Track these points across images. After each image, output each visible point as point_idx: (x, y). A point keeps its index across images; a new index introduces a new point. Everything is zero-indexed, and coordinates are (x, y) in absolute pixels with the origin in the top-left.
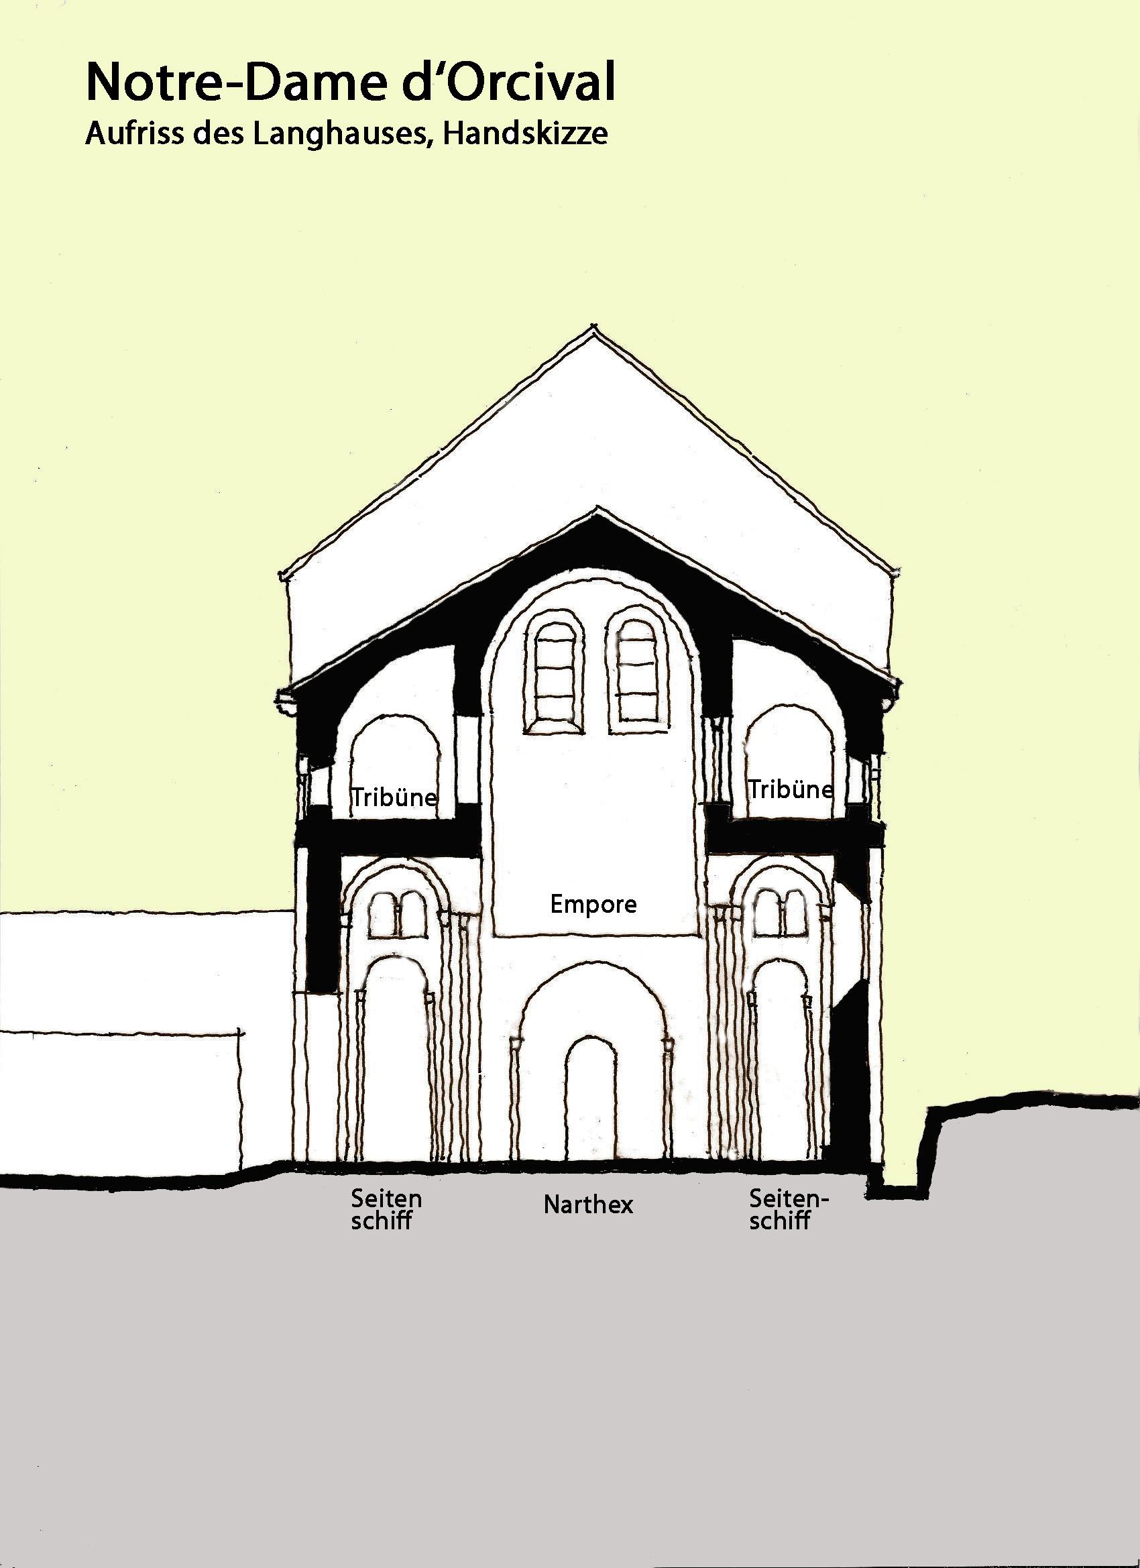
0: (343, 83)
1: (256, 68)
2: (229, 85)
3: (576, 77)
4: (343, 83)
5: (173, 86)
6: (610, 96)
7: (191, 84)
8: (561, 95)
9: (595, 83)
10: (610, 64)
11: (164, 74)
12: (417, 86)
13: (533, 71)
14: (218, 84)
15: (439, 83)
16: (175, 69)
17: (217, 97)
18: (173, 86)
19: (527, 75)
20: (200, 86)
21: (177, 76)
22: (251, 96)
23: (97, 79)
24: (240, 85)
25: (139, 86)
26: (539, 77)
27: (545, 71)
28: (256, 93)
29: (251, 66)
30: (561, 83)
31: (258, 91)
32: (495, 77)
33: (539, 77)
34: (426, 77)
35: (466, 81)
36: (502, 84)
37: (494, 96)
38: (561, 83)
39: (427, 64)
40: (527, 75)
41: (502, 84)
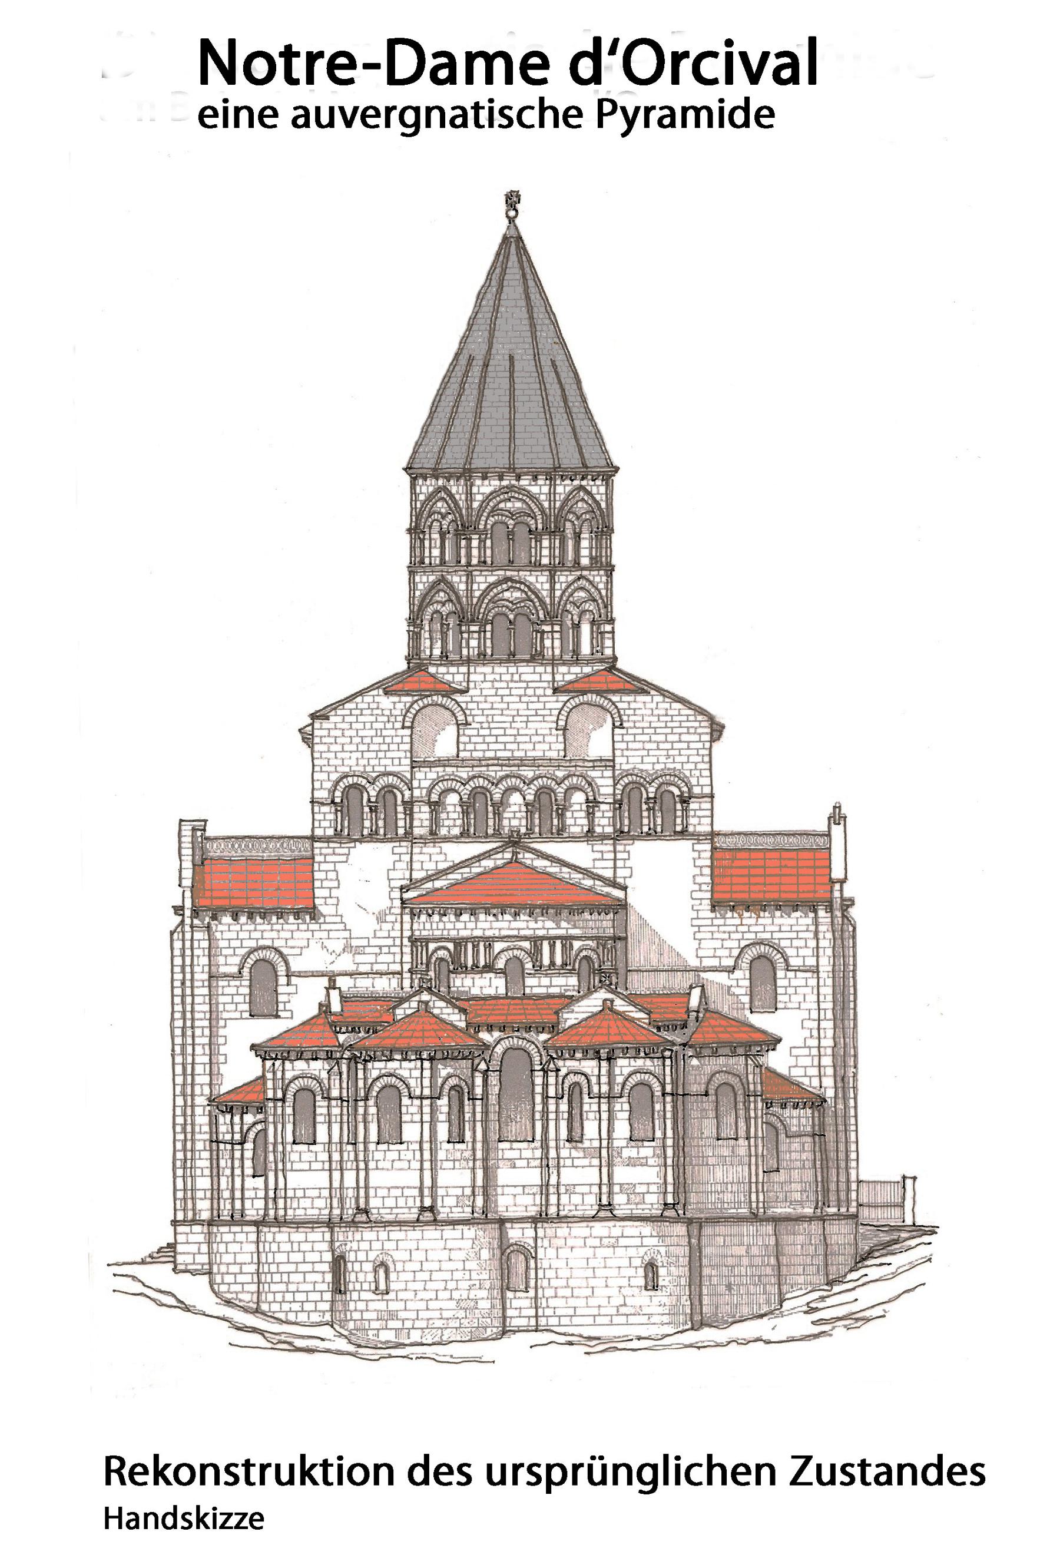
0: (499, 64)
1: (397, 47)
2: (367, 66)
3: (772, 57)
4: (499, 64)
5: (299, 67)
6: (812, 80)
7: (321, 66)
8: (754, 78)
9: (794, 65)
10: (812, 41)
11: (289, 54)
12: (586, 68)
13: (722, 50)
14: (352, 65)
15: (612, 64)
16: (302, 47)
17: (351, 81)
18: (299, 67)
19: (715, 55)
20: (332, 67)
21: (303, 56)
22: (392, 80)
23: (209, 57)
24: (377, 66)
25: (260, 67)
26: (729, 56)
27: (735, 50)
28: (397, 77)
29: (392, 44)
30: (755, 65)
31: (399, 75)
32: (678, 57)
33: (729, 56)
34: (596, 56)
35: (644, 62)
36: (686, 66)
37: (675, 80)
38: (755, 65)
39: (597, 41)
40: (715, 55)
41: (686, 66)
